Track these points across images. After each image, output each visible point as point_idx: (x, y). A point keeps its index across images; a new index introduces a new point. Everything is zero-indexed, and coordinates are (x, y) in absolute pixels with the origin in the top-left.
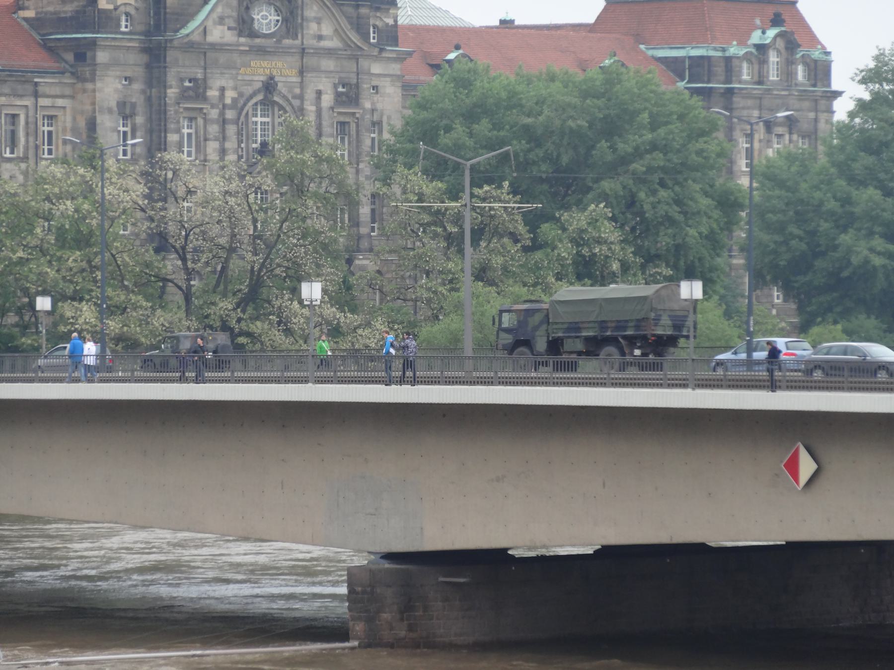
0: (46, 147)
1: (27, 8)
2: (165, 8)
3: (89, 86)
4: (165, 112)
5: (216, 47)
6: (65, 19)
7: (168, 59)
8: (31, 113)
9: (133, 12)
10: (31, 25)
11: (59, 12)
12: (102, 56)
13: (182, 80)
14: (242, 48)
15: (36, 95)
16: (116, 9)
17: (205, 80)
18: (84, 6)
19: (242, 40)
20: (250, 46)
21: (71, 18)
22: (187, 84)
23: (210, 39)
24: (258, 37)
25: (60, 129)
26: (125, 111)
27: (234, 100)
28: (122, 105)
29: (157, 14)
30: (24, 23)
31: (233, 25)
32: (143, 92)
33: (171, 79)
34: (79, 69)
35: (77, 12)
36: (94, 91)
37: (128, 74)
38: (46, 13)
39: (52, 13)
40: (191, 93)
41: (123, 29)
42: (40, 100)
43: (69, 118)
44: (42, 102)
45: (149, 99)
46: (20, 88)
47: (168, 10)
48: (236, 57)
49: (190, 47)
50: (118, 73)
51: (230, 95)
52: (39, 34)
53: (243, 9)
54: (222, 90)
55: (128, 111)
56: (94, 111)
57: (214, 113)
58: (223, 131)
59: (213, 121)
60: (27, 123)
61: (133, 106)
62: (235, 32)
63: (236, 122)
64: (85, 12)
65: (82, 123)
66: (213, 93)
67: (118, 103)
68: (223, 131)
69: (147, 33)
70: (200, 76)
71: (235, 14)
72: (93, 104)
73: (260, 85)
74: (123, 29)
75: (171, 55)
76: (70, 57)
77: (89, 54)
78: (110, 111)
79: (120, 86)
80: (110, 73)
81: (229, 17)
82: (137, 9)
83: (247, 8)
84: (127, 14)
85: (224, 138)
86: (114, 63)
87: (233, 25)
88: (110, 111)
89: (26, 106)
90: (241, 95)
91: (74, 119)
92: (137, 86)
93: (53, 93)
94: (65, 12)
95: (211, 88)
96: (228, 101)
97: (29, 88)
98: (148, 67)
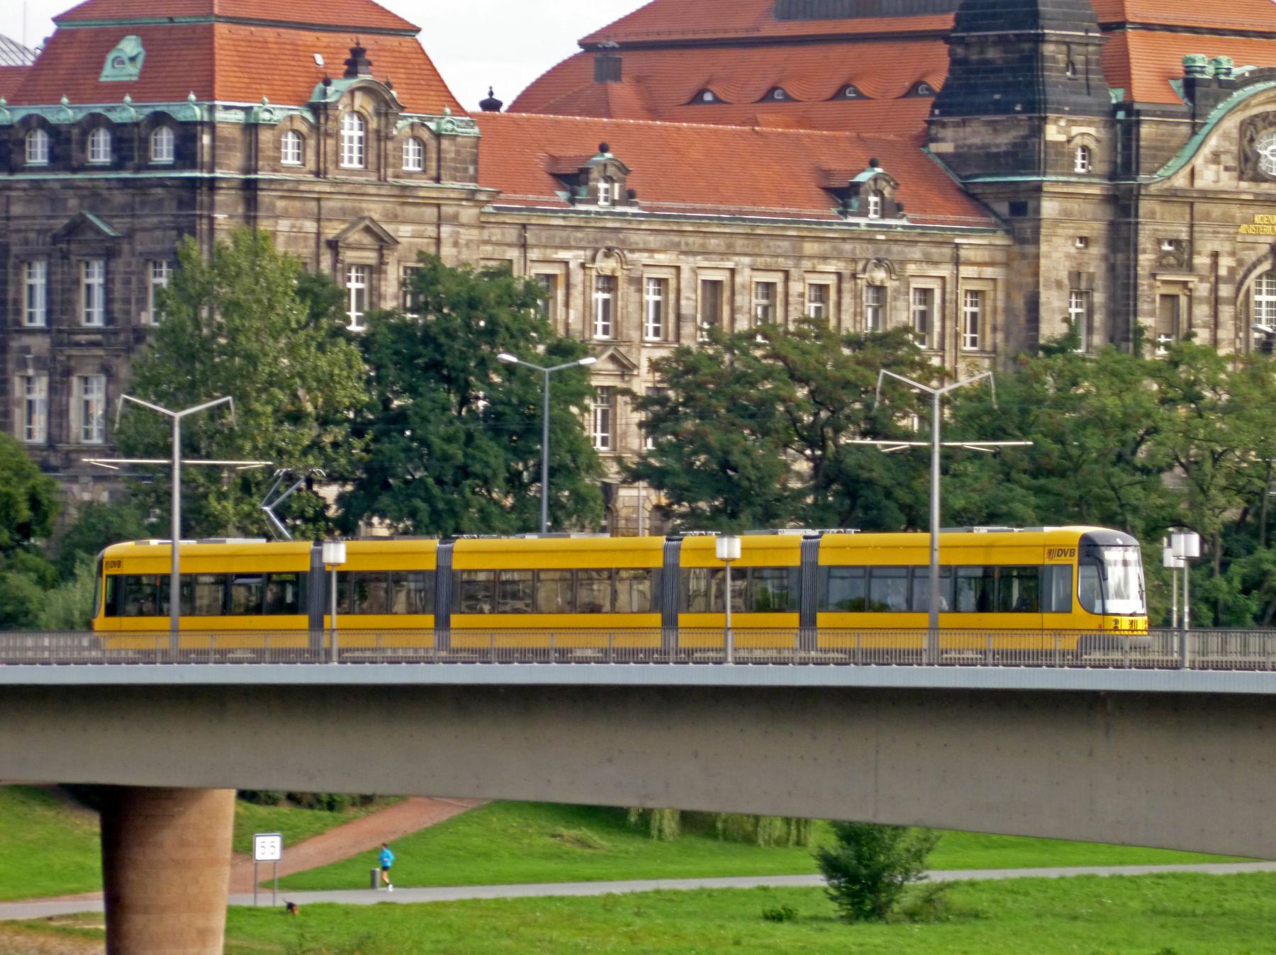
0: (969, 336)
1: (943, 140)
2: (1138, 140)
3: (1030, 249)
4: (1136, 286)
5: (1208, 196)
6: (997, 155)
7: (1141, 212)
8: (949, 288)
9: (1092, 145)
10: (948, 164)
11: (988, 146)
12: (1049, 208)
13: (1159, 242)
14: (1244, 197)
15: (957, 262)
16: (1069, 141)
17: (1191, 241)
18: (1024, 137)
19: (1244, 185)
20: (1256, 194)
21: (1006, 154)
22: (1166, 247)
23: (1199, 184)
24: (1266, 180)
25: (988, 309)
26: (1078, 286)
27: (1232, 270)
28: (1076, 276)
29: (1127, 147)
30: (938, 161)
31: (1232, 163)
32: (1105, 258)
33: (1145, 240)
34: (1017, 225)
35: (1014, 145)
36: (1037, 256)
37: (1085, 233)
38: (970, 147)
39: (979, 147)
40: (1172, 260)
41: (1079, 170)
42: (962, 268)
43: (1001, 295)
44: (965, 271)
45: (1112, 269)
46: (935, 251)
47: (1142, 143)
48: (1236, 211)
49: (1170, 197)
50: (1071, 232)
51: (1225, 263)
52: (960, 177)
53: (1245, 142)
54: (1215, 255)
55: (1083, 285)
56: (1037, 284)
57: (1203, 289)
58: (1215, 315)
59: (1201, 300)
60: (943, 301)
61: (1091, 277)
62: (1235, 174)
63: (1233, 301)
64: (1026, 145)
65: (1020, 303)
66: (1202, 261)
67: (1070, 273)
68: (1215, 315)
69: (1112, 176)
70: (1184, 236)
71: (1234, 148)
72: (1036, 274)
73: (1264, 249)
74: (1079, 170)
75: (1145, 206)
76: (1003, 208)
77: (1031, 205)
78: (1059, 285)
79: (1073, 250)
80: (1060, 231)
81: (1225, 152)
82: (1098, 140)
83: (1252, 140)
84: (1085, 148)
85: (1215, 325)
86: (1067, 216)
87: (1232, 163)
88: (1059, 285)
89: (943, 278)
90: (1240, 263)
91: (1008, 296)
92: (1096, 250)
93: (979, 259)
94: (997, 145)
95: (1199, 253)
96: (1223, 272)
97: (947, 251)
98: (1113, 226)
